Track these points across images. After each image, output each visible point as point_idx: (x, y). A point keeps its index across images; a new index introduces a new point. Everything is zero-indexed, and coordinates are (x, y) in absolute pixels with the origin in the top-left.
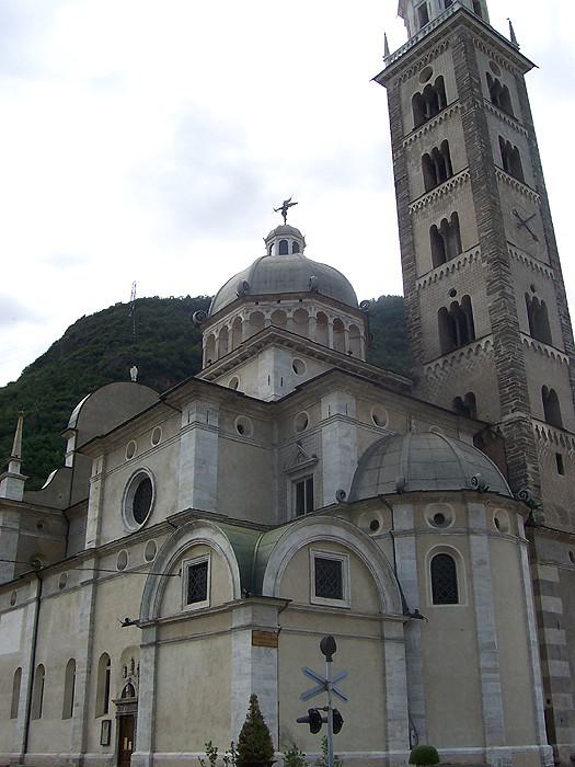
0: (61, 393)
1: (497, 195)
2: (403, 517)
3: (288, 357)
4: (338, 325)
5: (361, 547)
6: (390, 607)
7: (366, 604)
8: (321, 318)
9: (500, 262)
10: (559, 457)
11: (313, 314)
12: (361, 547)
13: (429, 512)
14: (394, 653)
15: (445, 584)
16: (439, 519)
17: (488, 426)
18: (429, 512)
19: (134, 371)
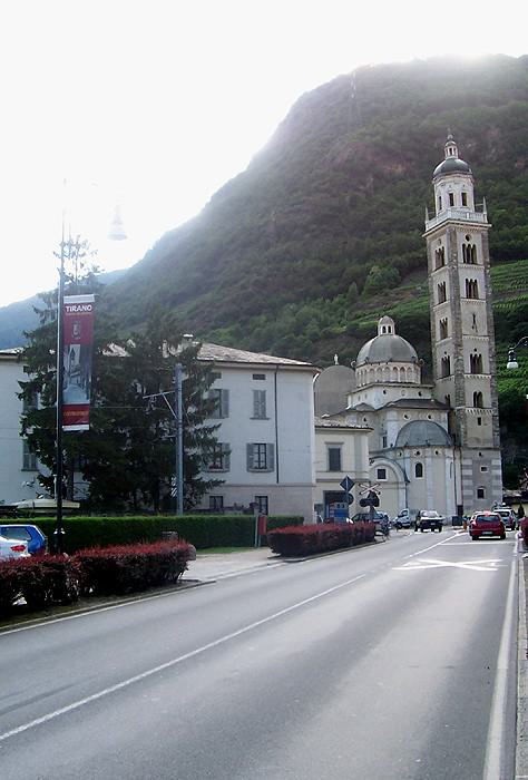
0: (295, 195)
1: (459, 314)
2: (407, 453)
3: (381, 390)
4: (402, 369)
5: (392, 466)
6: (401, 479)
7: (393, 480)
8: (395, 368)
9: (458, 345)
10: (479, 419)
11: (392, 369)
12: (392, 466)
13: (415, 452)
14: (402, 493)
15: (419, 471)
16: (418, 453)
17: (452, 409)
18: (415, 452)
19: (336, 358)
